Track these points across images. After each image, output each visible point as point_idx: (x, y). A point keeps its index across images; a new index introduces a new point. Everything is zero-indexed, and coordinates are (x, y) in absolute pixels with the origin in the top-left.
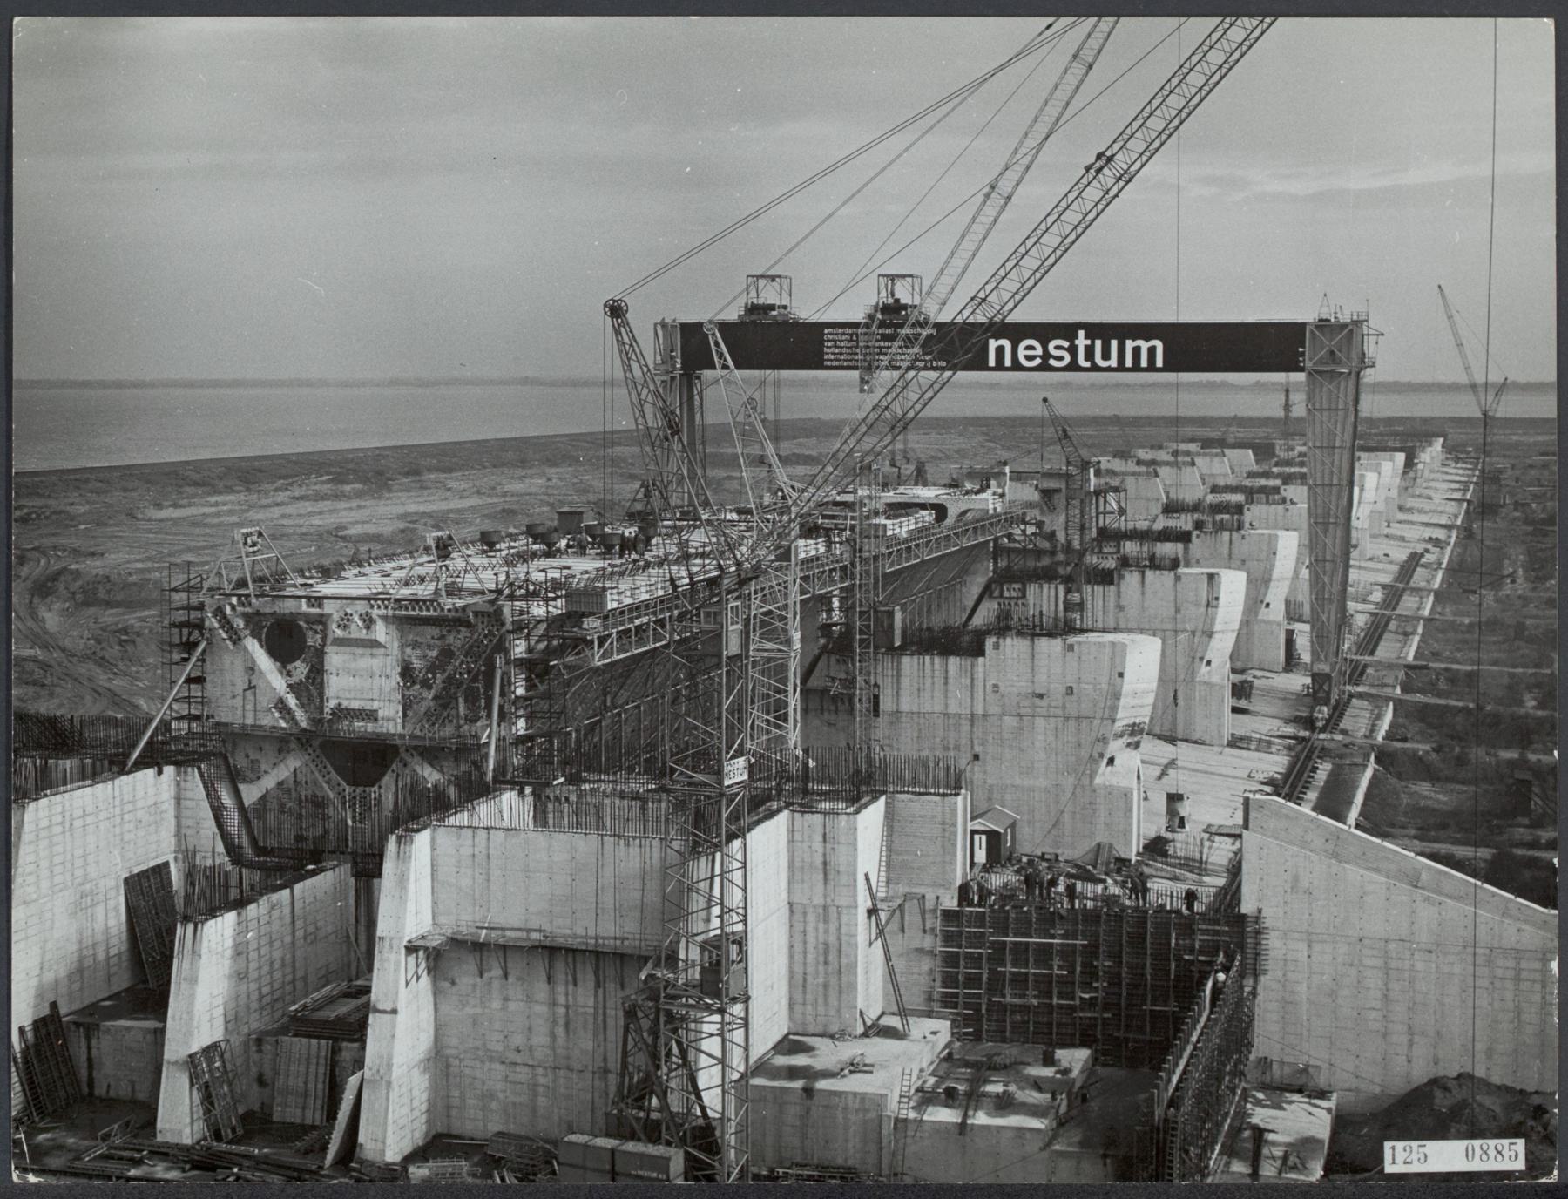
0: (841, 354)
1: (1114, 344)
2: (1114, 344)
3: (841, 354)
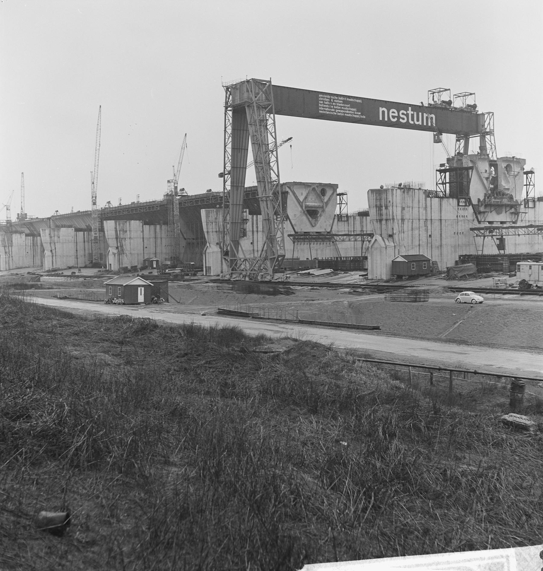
0: (326, 108)
1: (420, 114)
2: (420, 114)
3: (326, 108)
